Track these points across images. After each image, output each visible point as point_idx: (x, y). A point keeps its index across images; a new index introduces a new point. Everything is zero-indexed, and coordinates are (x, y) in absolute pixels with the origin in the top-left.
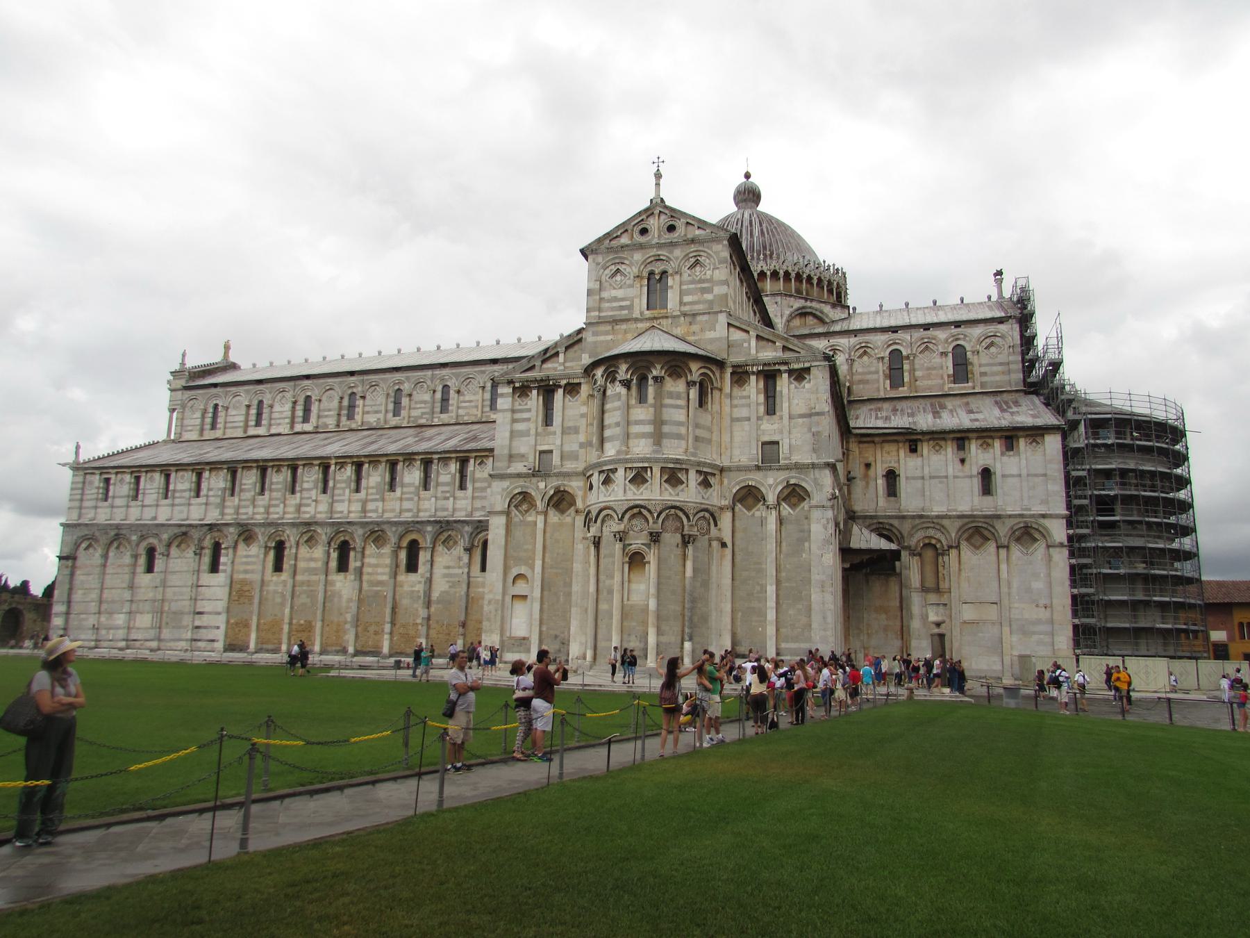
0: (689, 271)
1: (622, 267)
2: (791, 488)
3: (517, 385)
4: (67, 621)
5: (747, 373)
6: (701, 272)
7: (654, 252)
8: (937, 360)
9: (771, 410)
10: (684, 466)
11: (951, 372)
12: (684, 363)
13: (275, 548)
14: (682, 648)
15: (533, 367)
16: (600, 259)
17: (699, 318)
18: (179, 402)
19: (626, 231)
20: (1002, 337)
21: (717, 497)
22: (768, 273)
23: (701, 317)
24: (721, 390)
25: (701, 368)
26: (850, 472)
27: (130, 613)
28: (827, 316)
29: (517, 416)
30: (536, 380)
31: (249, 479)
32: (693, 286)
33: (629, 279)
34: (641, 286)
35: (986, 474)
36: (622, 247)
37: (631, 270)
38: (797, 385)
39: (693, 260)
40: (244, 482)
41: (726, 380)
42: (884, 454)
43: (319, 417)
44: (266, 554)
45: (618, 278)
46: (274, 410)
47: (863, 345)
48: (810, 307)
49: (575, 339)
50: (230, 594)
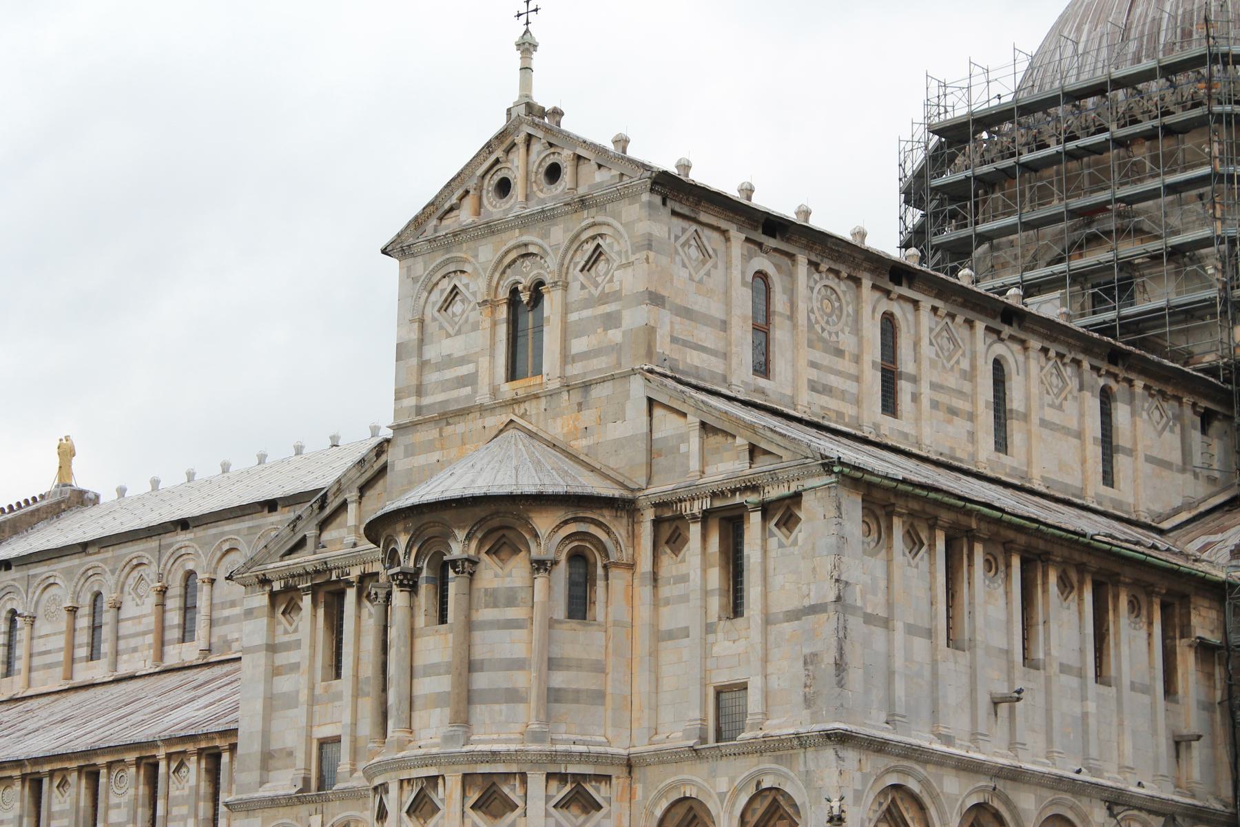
0: (581, 277)
1: (460, 281)
2: (770, 799)
3: (277, 586)
5: (681, 517)
6: (606, 274)
7: (514, 238)
9: (736, 607)
10: (514, 768)
12: (520, 518)
15: (300, 544)
16: (420, 267)
17: (596, 392)
19: (467, 192)
23: (599, 387)
24: (631, 566)
25: (566, 522)
29: (282, 658)
30: (307, 573)
32: (587, 313)
33: (474, 309)
34: (494, 324)
36: (455, 235)
37: (475, 286)
38: (784, 540)
39: (590, 247)
41: (643, 541)
43: (212, 623)
45: (457, 307)
46: (124, 614)
49: (377, 466)
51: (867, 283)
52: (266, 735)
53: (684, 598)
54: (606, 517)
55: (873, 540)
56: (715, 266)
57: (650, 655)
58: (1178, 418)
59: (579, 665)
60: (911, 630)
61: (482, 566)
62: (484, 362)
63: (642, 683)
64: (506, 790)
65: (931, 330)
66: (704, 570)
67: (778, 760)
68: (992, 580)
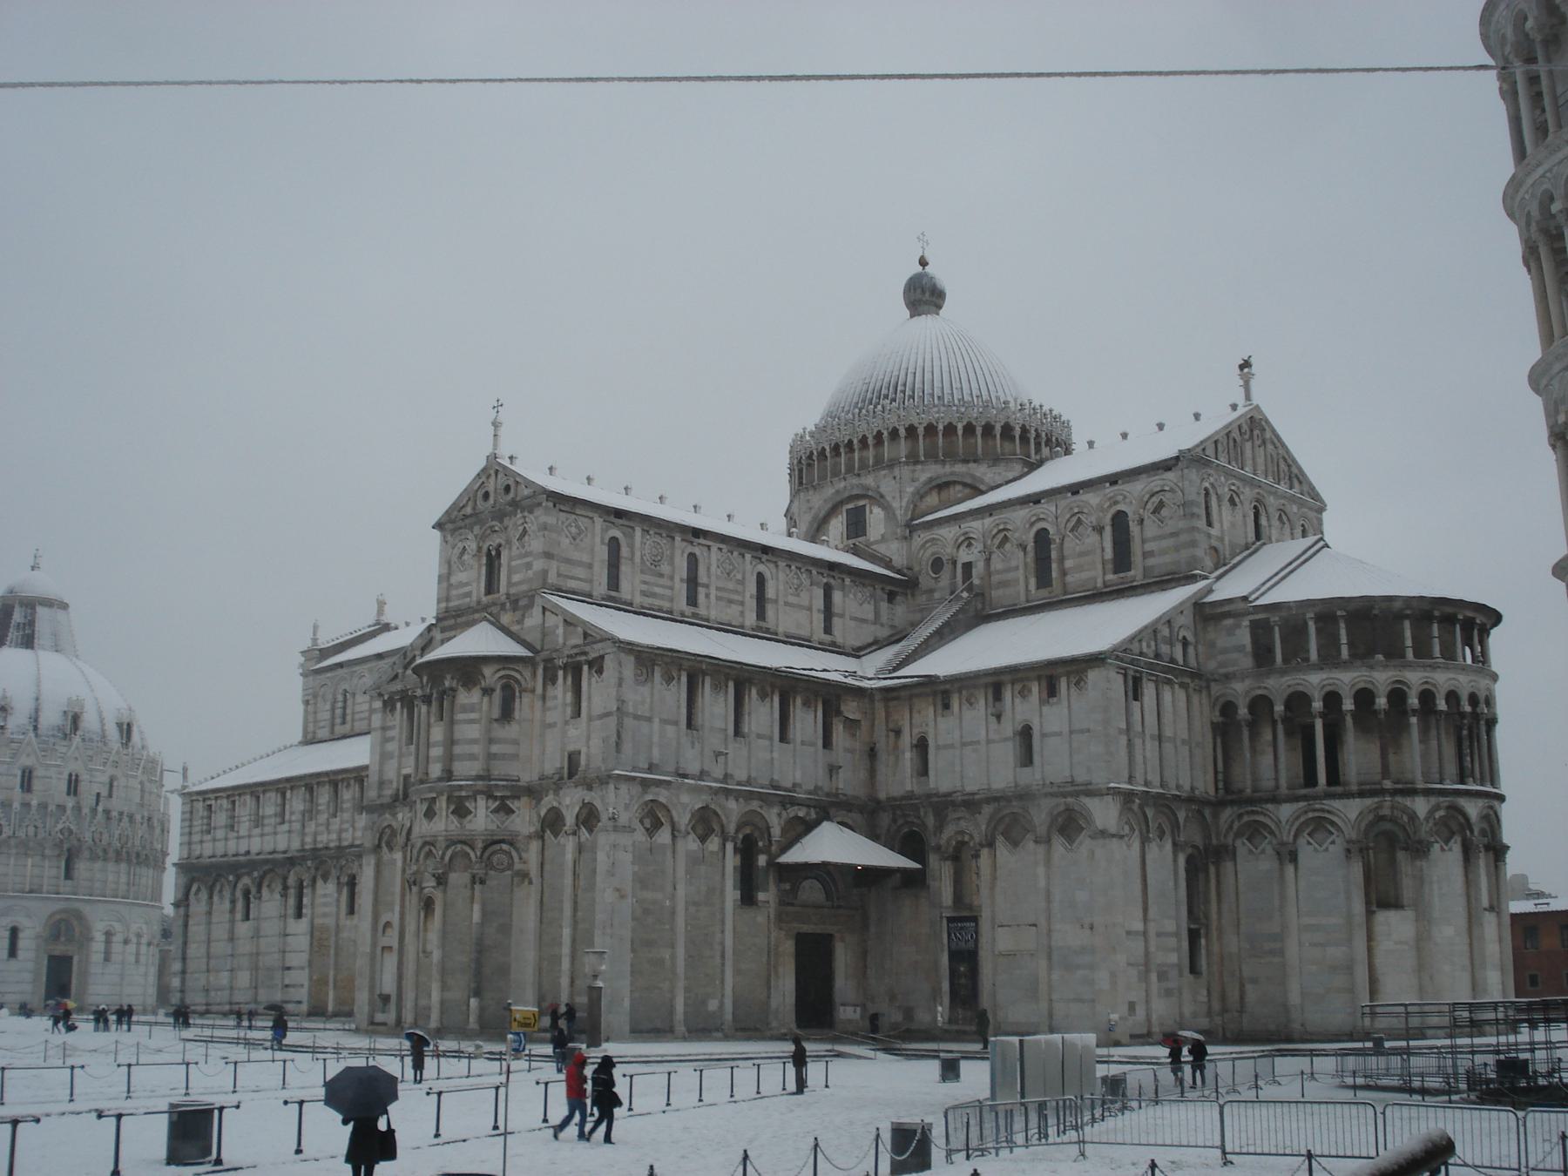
4: (183, 981)
8: (1092, 539)
9: (577, 713)
11: (1109, 554)
13: (347, 884)
14: (468, 1006)
18: (311, 691)
19: (469, 499)
20: (1172, 490)
21: (524, 820)
22: (885, 434)
24: (533, 691)
25: (499, 670)
27: (232, 970)
28: (982, 482)
29: (390, 734)
31: (324, 796)
32: (519, 562)
34: (480, 566)
35: (1026, 733)
39: (521, 528)
40: (320, 801)
42: (915, 715)
44: (339, 892)
47: (1001, 527)
48: (952, 474)
50: (311, 944)
51: (678, 539)
52: (381, 771)
54: (520, 667)
58: (872, 596)
60: (664, 722)
61: (458, 692)
62: (475, 585)
64: (467, 804)
65: (718, 560)
66: (565, 693)
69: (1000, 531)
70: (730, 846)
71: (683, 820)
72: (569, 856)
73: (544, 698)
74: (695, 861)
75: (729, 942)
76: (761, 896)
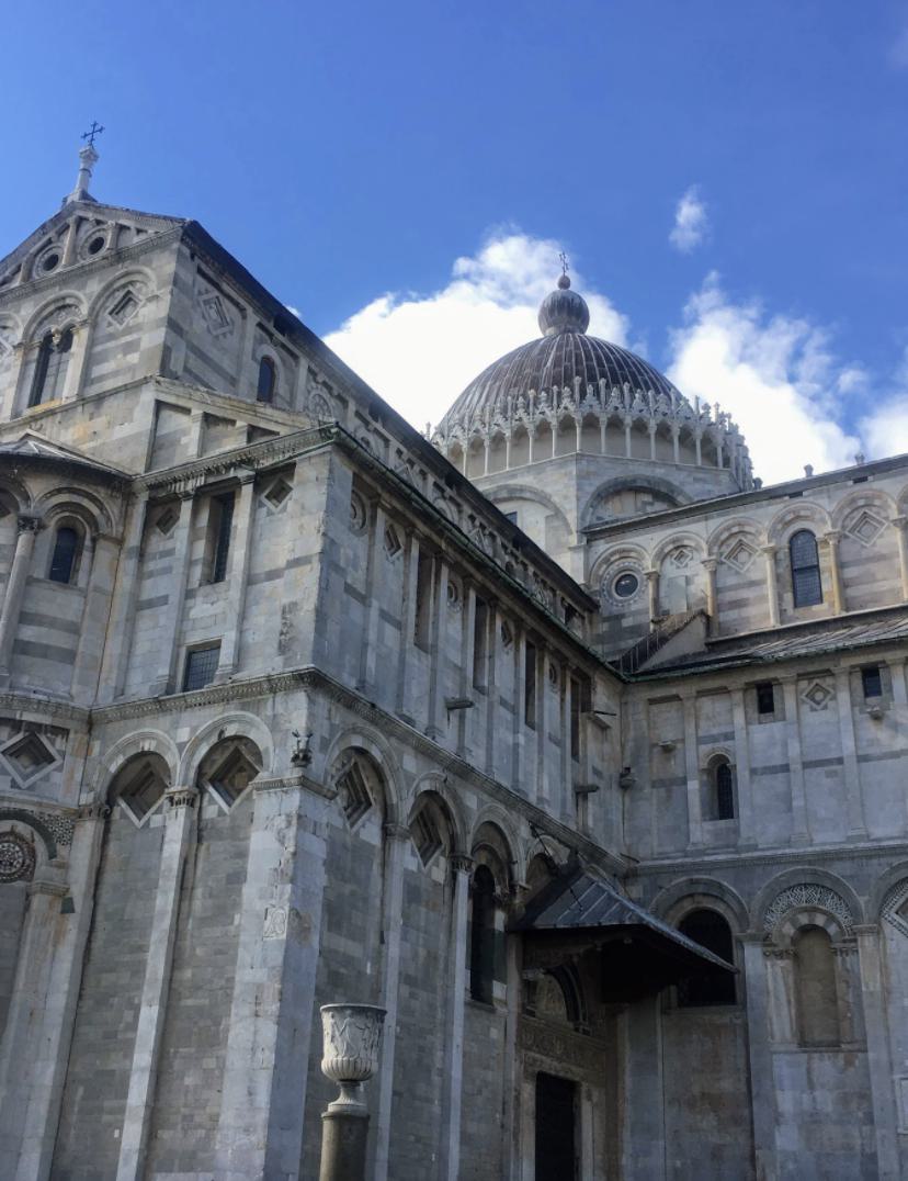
0: (110, 318)
2: (232, 748)
9: (217, 570)
24: (120, 542)
25: (59, 491)
26: (628, 769)
34: (25, 364)
38: (272, 507)
39: (120, 294)
41: (134, 521)
47: (735, 530)
53: (167, 570)
54: (101, 493)
55: (358, 523)
56: (231, 333)
57: (127, 620)
59: (52, 623)
63: (115, 646)
66: (192, 542)
67: (244, 707)
68: (453, 605)
69: (732, 535)
70: (463, 879)
71: (405, 808)
72: (173, 849)
73: (142, 554)
74: (412, 894)
75: (456, 1073)
76: (498, 990)
